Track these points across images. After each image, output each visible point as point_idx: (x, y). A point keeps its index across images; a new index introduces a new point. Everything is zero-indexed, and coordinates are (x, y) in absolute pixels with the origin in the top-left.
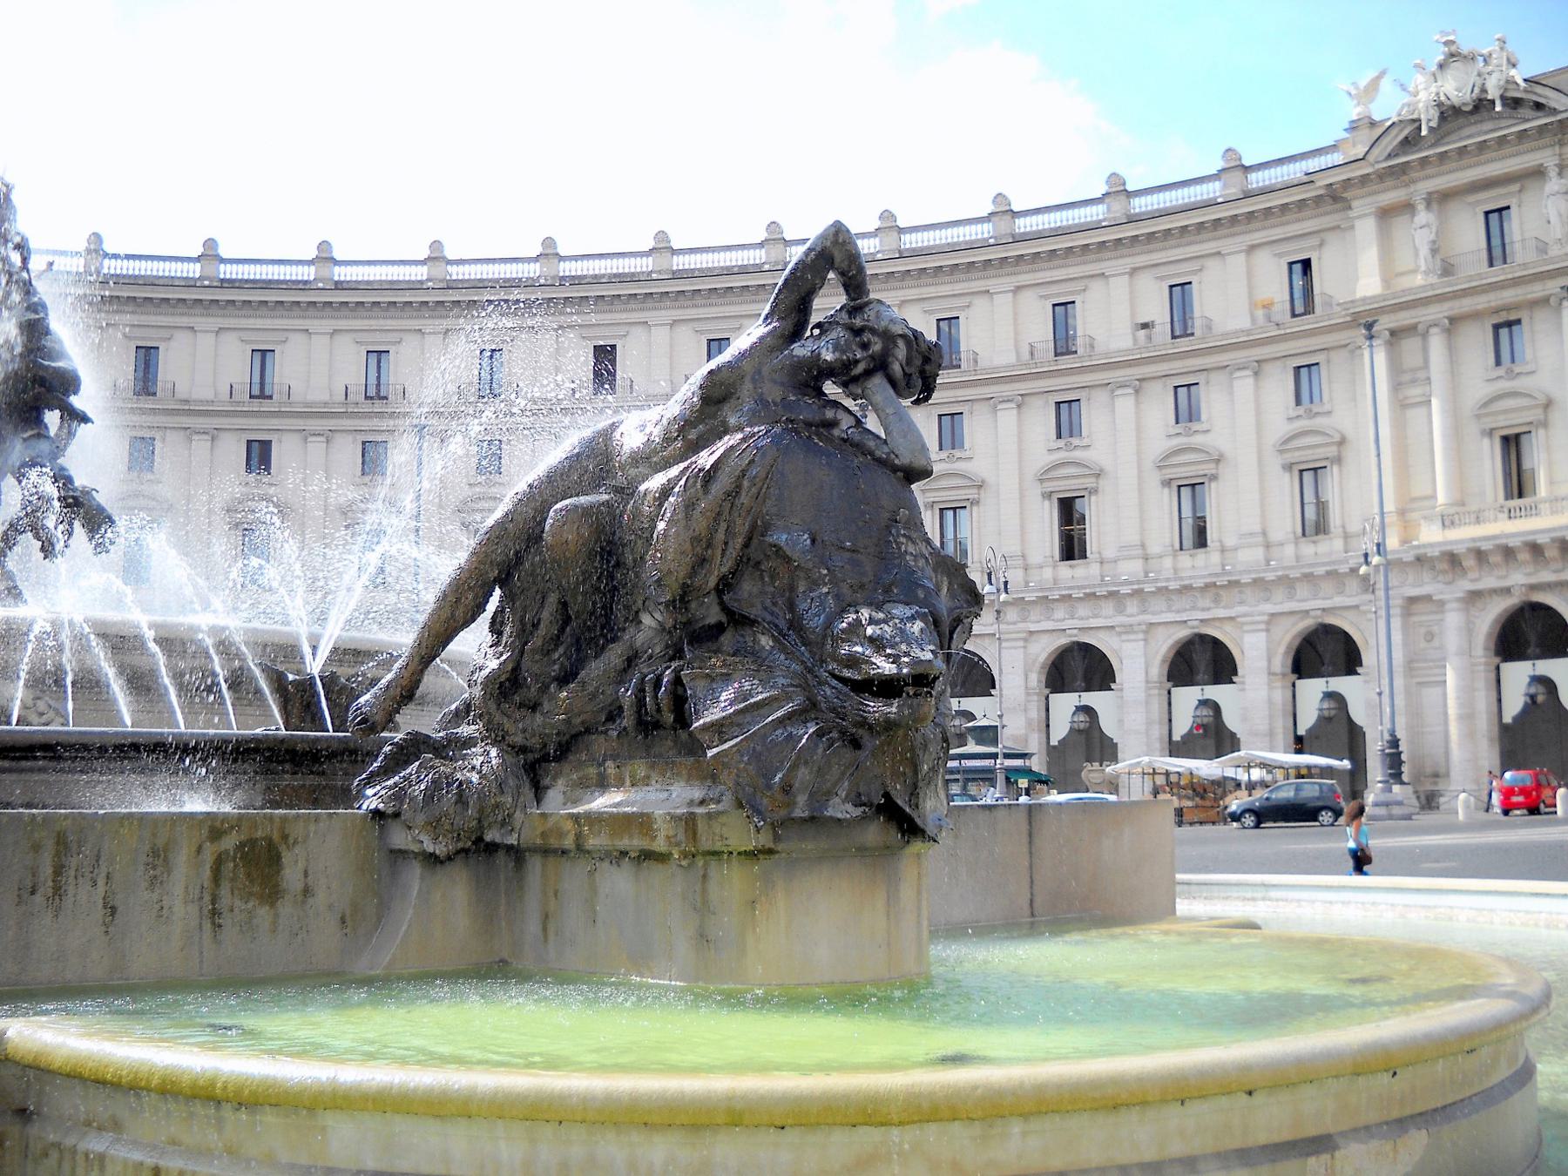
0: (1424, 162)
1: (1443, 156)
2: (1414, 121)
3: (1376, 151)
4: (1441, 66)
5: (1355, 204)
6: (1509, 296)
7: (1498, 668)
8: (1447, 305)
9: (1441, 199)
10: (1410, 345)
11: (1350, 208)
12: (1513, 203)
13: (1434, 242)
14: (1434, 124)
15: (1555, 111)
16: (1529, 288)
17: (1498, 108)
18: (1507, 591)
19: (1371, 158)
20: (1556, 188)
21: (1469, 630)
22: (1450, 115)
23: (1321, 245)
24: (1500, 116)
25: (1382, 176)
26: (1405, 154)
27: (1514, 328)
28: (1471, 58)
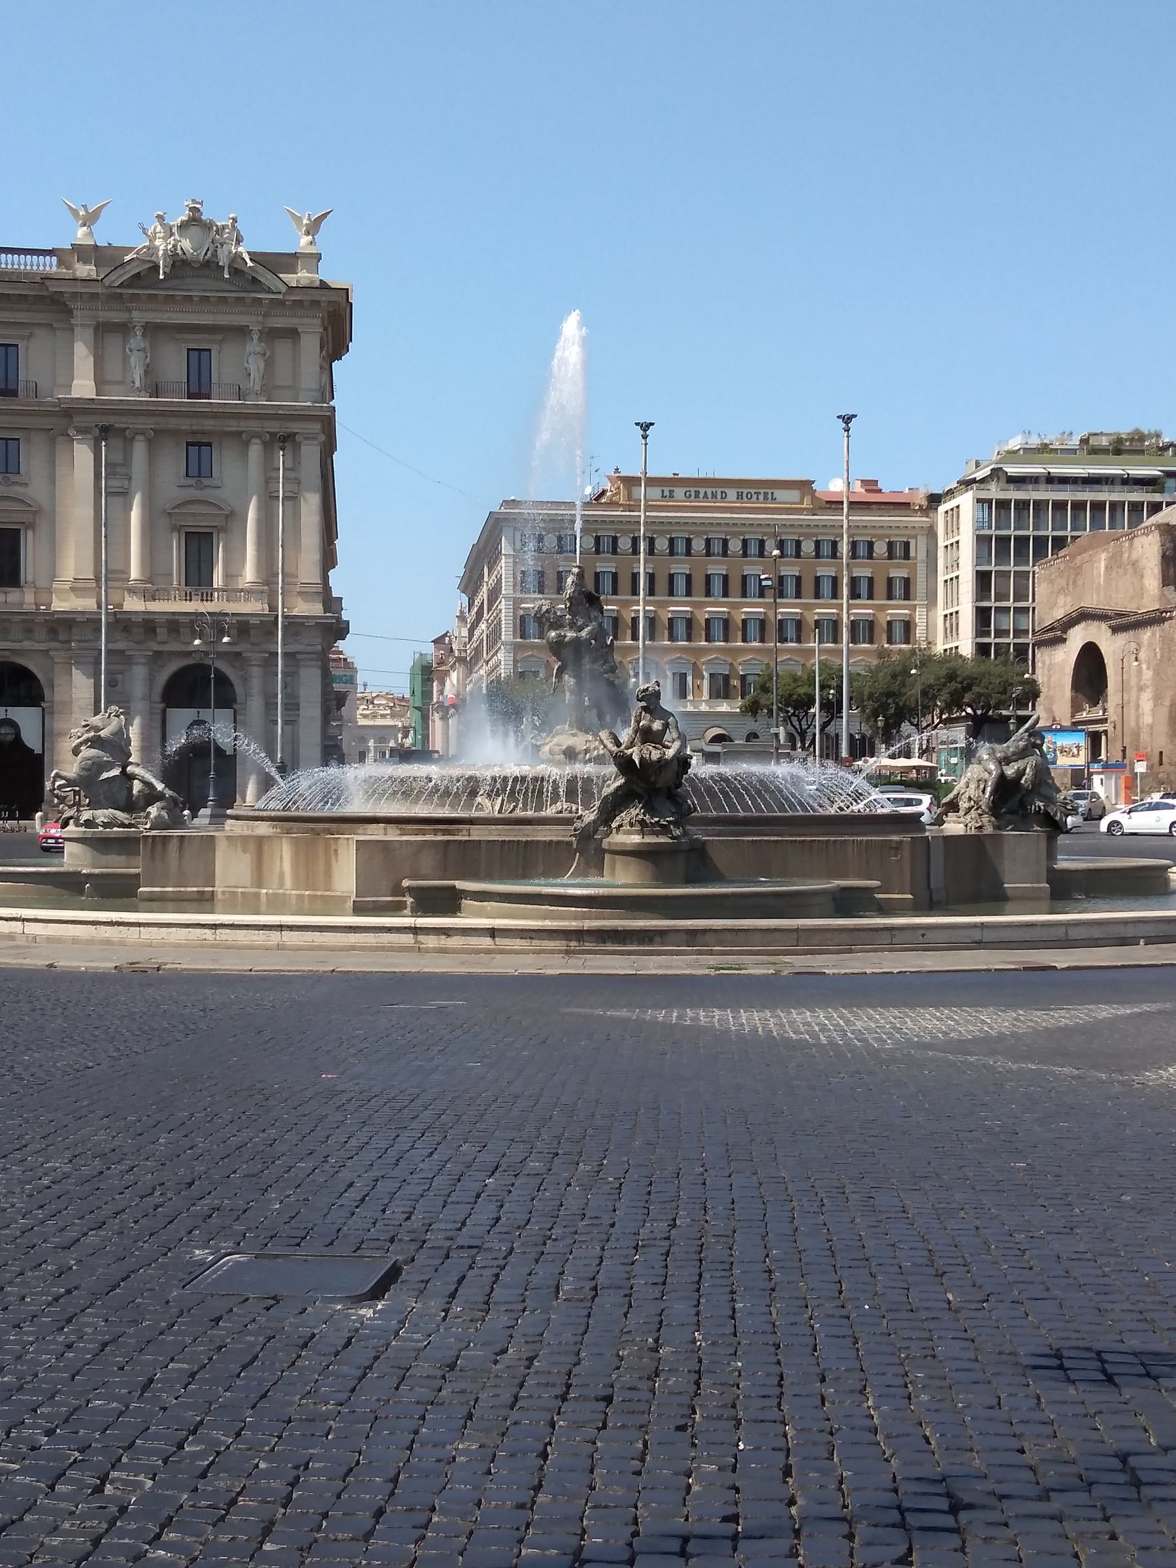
4: (183, 226)
6: (209, 424)
7: (164, 712)
8: (153, 420)
13: (148, 365)
15: (270, 291)
18: (189, 654)
19: (107, 282)
20: (258, 349)
21: (151, 681)
22: (179, 263)
28: (208, 226)
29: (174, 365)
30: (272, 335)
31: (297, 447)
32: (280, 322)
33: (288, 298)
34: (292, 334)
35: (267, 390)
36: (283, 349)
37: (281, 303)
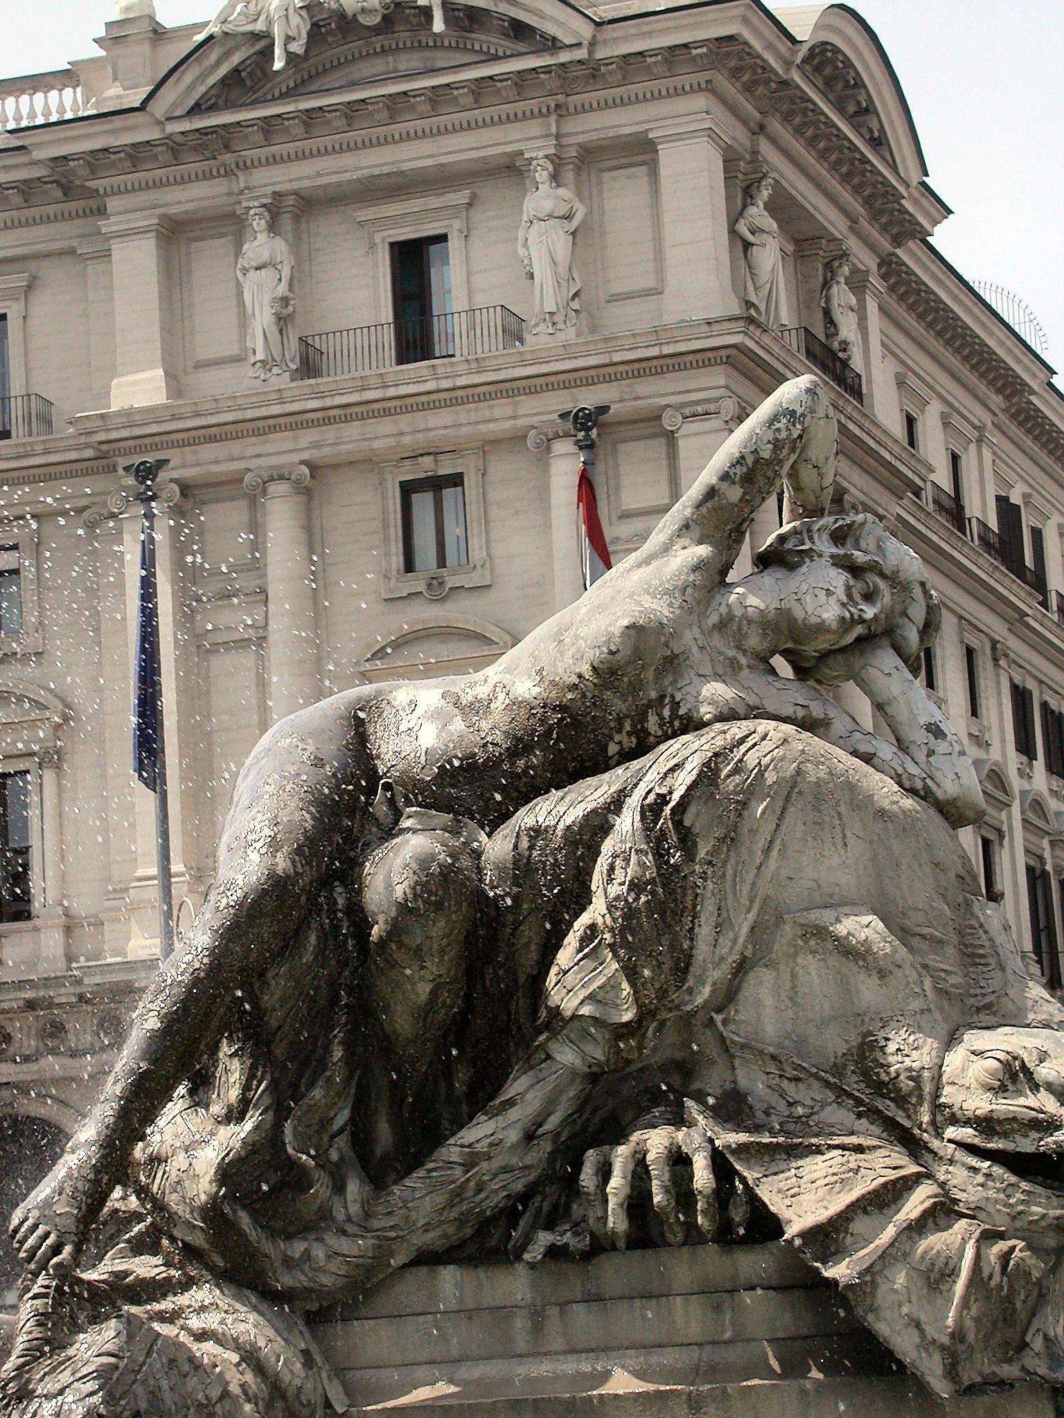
0: (269, 127)
1: (311, 118)
2: (256, 36)
3: (169, 96)
5: (113, 204)
8: (307, 437)
9: (297, 212)
10: (225, 518)
11: (101, 212)
12: (453, 229)
13: (285, 301)
14: (297, 47)
15: (553, 45)
16: (484, 410)
17: (438, 26)
19: (159, 108)
20: (548, 206)
23: (29, 288)
24: (437, 44)
25: (175, 148)
26: (230, 106)
27: (448, 494)
29: (361, 295)
30: (586, 163)
31: (670, 438)
32: (592, 126)
33: (600, 54)
34: (641, 152)
35: (581, 303)
36: (623, 194)
37: (593, 71)
